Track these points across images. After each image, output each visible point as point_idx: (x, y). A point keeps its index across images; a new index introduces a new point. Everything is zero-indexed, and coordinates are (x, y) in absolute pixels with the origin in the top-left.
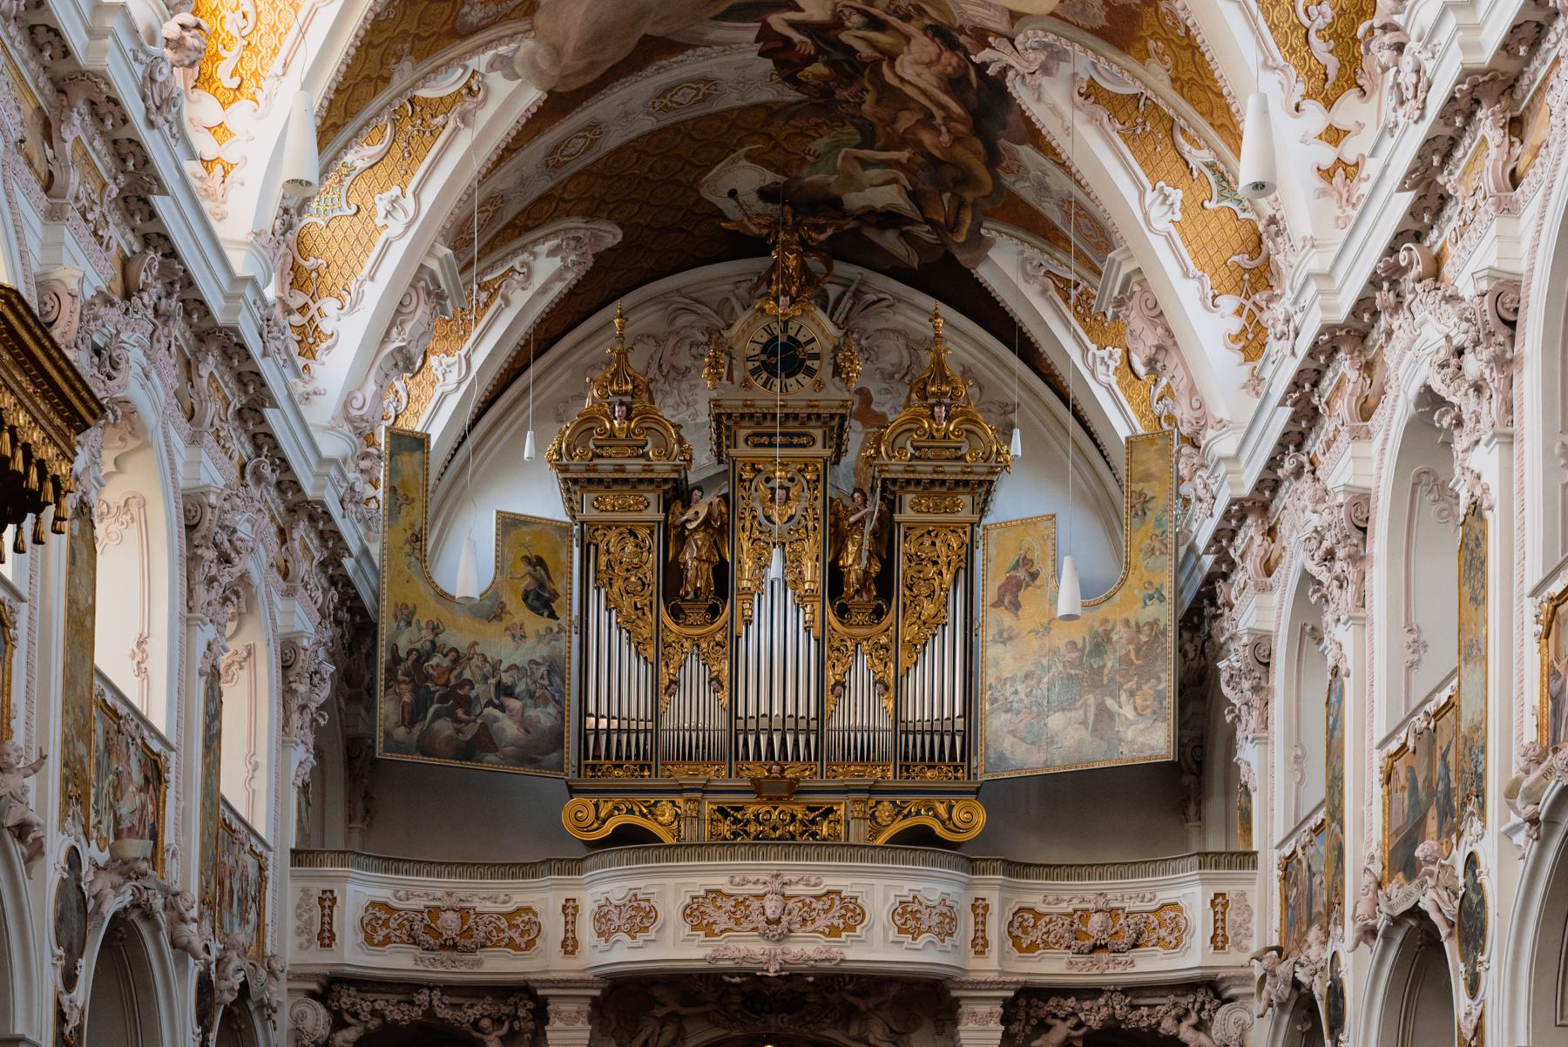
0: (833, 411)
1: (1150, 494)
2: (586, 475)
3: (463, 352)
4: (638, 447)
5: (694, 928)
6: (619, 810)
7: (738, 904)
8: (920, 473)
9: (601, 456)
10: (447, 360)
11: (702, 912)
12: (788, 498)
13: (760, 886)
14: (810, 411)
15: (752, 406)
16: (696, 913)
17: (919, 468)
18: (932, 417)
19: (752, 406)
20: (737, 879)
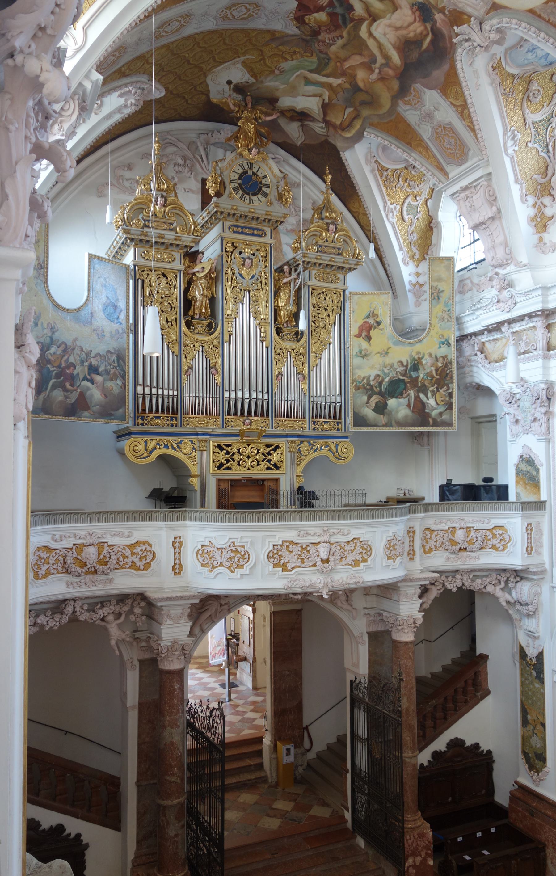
0: (279, 219)
1: (441, 289)
2: (140, 238)
5: (275, 566)
6: (160, 445)
7: (303, 549)
8: (323, 260)
11: (281, 556)
12: (252, 265)
13: (317, 537)
14: (266, 217)
15: (236, 209)
16: (276, 556)
17: (323, 258)
18: (328, 230)
19: (236, 209)
20: (302, 533)
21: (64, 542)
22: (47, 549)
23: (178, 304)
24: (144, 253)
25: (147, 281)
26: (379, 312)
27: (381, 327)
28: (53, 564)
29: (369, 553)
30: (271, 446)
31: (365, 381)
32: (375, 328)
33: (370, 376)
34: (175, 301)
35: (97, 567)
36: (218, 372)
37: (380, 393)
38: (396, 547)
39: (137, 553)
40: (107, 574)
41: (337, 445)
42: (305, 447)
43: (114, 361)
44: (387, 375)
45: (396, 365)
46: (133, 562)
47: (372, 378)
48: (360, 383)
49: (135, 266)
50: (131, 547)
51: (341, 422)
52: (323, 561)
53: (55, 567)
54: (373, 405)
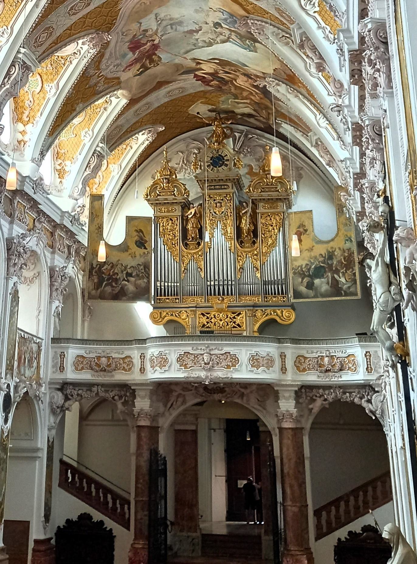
2: (155, 202)
3: (119, 163)
4: (172, 192)
5: (180, 366)
9: (160, 195)
10: (114, 165)
16: (181, 360)
21: (91, 355)
22: (82, 357)
23: (178, 234)
24: (159, 209)
25: (161, 225)
26: (306, 223)
27: (307, 233)
28: (85, 365)
29: (236, 362)
30: (235, 313)
31: (300, 268)
32: (304, 234)
33: (302, 265)
34: (177, 232)
35: (106, 368)
36: (202, 270)
37: (309, 276)
38: (259, 360)
39: (126, 363)
40: (111, 372)
41: (282, 312)
42: (259, 314)
43: (142, 269)
44: (312, 264)
45: (318, 256)
46: (124, 367)
47: (303, 266)
48: (296, 270)
49: (155, 217)
50: (123, 359)
51: (286, 297)
52: (205, 364)
53: (86, 366)
54: (306, 284)
